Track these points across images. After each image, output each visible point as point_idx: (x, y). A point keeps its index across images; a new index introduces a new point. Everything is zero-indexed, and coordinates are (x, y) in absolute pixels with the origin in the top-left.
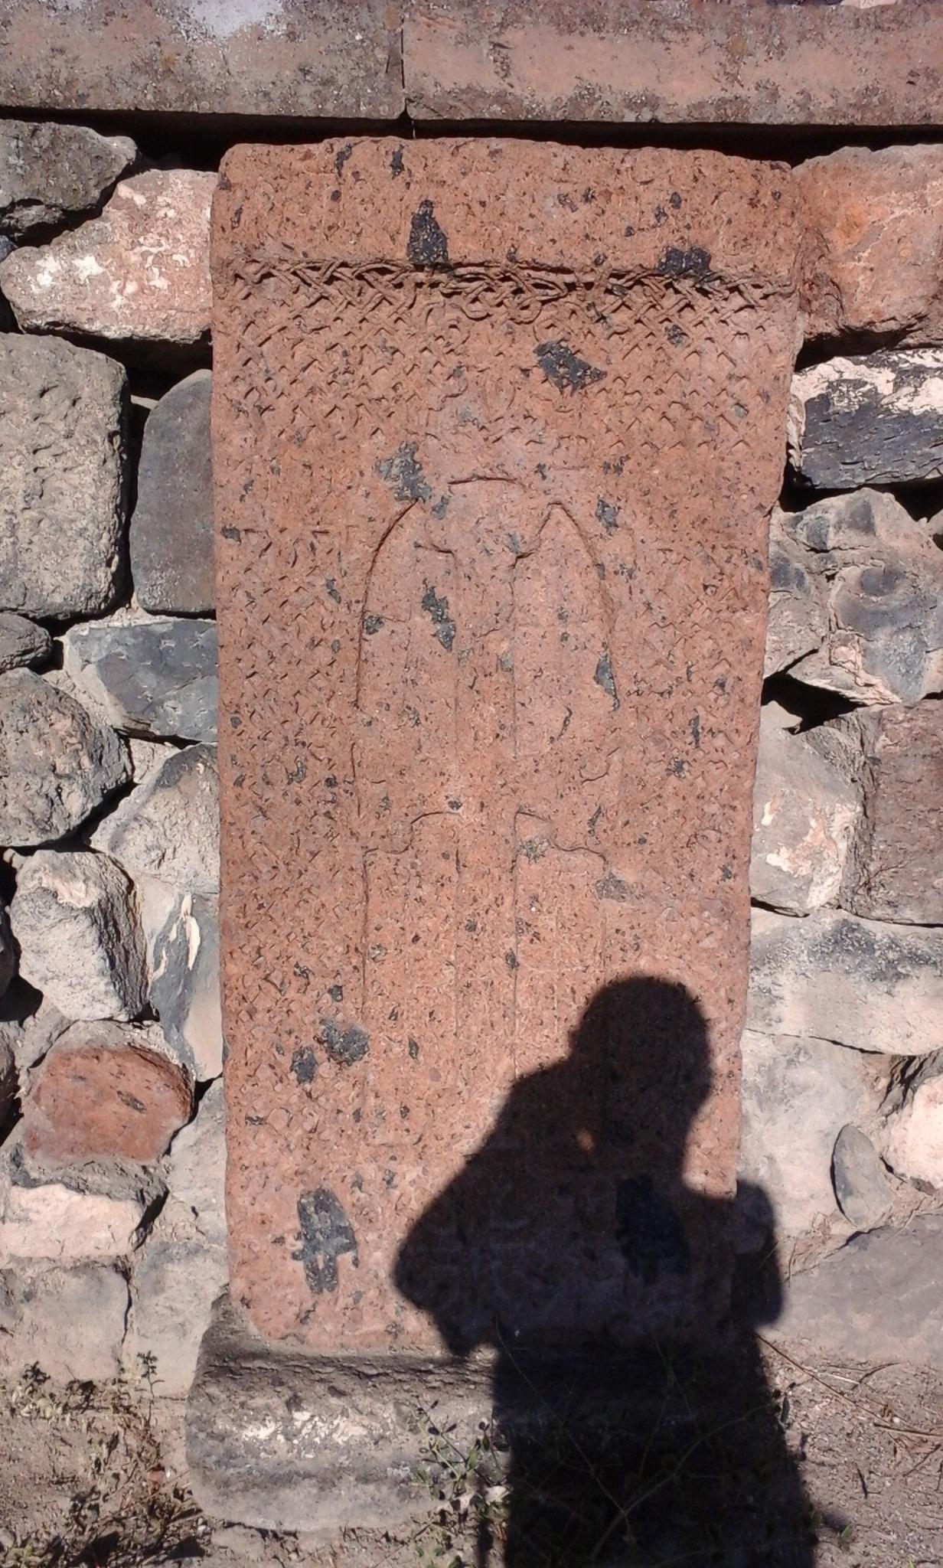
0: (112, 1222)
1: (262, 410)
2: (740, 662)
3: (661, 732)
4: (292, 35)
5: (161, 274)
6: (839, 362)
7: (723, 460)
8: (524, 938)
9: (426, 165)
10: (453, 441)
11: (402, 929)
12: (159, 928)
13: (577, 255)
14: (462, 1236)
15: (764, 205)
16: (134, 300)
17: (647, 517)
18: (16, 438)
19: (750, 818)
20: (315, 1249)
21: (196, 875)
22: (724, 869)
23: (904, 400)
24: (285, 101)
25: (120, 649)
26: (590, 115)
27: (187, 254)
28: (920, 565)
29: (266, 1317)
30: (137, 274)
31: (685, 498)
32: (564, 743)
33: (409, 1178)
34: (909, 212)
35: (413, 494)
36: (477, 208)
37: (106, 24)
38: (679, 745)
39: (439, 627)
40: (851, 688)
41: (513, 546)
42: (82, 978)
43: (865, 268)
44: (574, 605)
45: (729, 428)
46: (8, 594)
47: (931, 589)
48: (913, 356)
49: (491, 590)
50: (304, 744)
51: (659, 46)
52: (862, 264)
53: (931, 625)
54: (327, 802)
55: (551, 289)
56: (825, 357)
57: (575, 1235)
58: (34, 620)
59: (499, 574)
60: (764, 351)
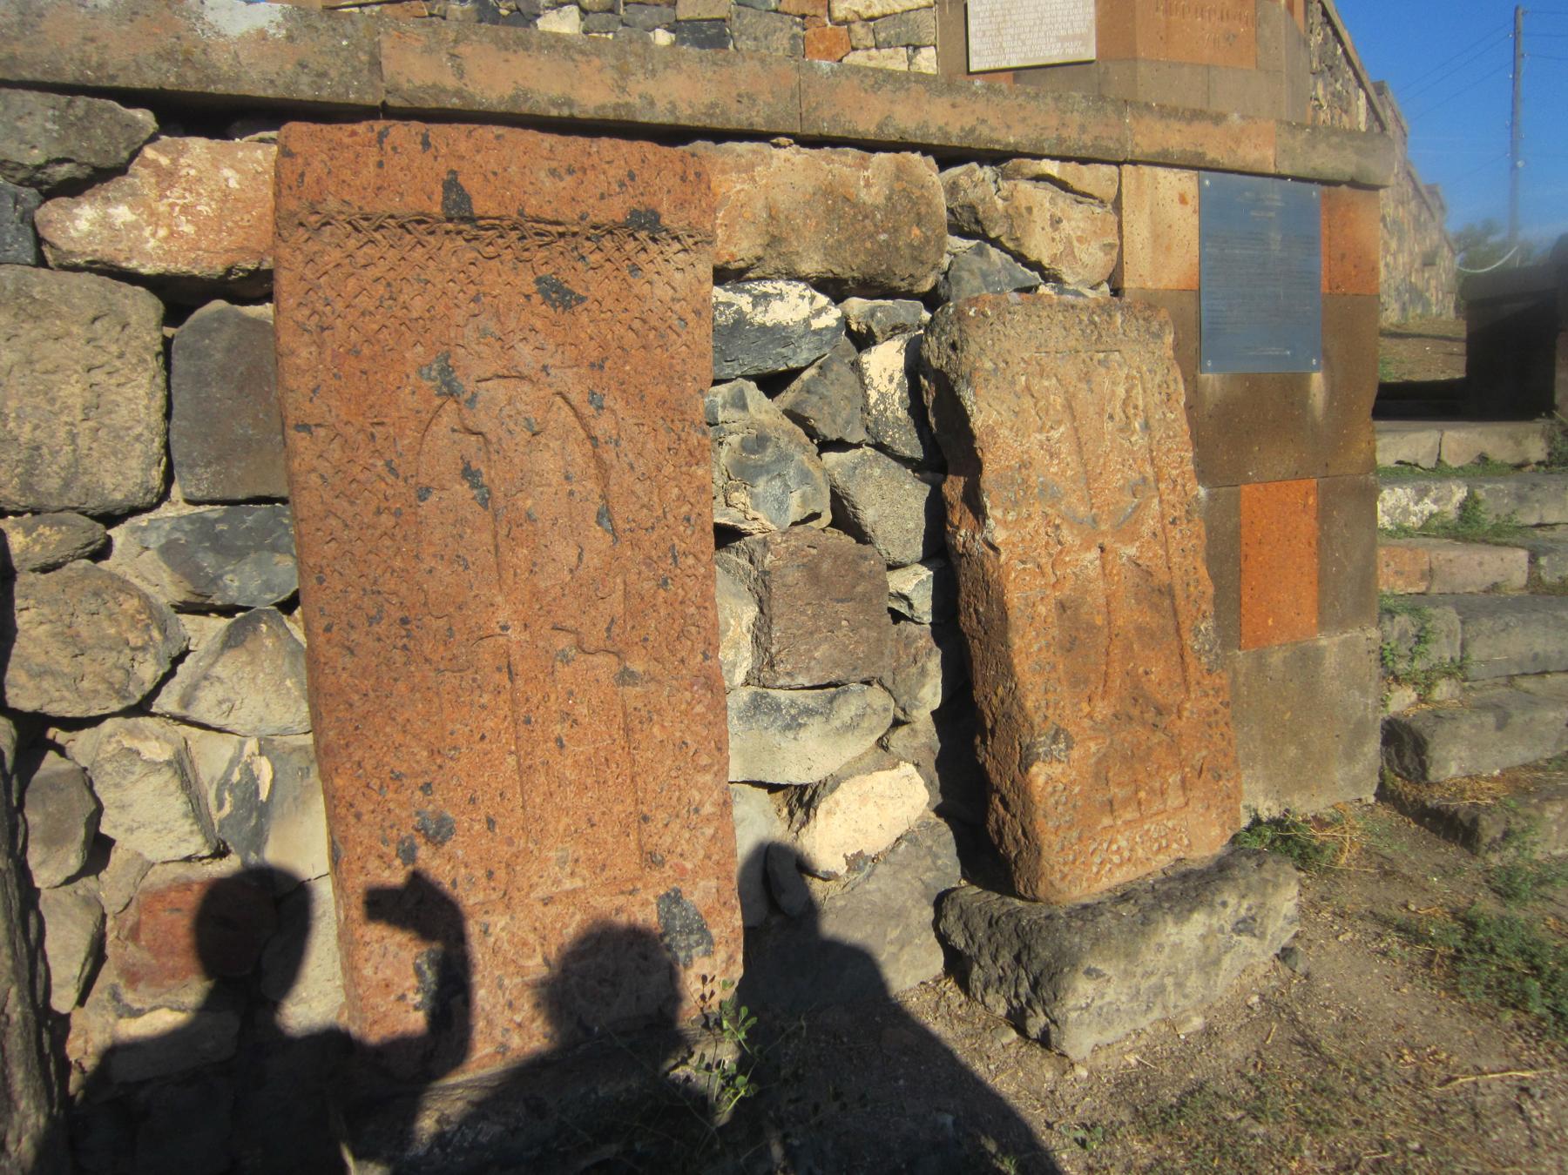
1: (323, 329)
3: (650, 558)
4: (290, 38)
5: (188, 221)
12: (219, 774)
16: (167, 243)
18: (72, 359)
19: (716, 616)
21: (261, 720)
22: (704, 653)
24: (287, 87)
25: (177, 535)
27: (210, 206)
30: (167, 221)
32: (581, 572)
33: (500, 925)
34: (746, 187)
35: (450, 391)
36: (491, 177)
37: (131, 21)
38: (664, 566)
39: (475, 492)
40: (742, 522)
41: (529, 425)
45: (675, 336)
46: (70, 495)
49: (516, 461)
50: (379, 592)
51: (570, 64)
54: (403, 637)
58: (92, 517)
59: (521, 449)
60: (694, 282)
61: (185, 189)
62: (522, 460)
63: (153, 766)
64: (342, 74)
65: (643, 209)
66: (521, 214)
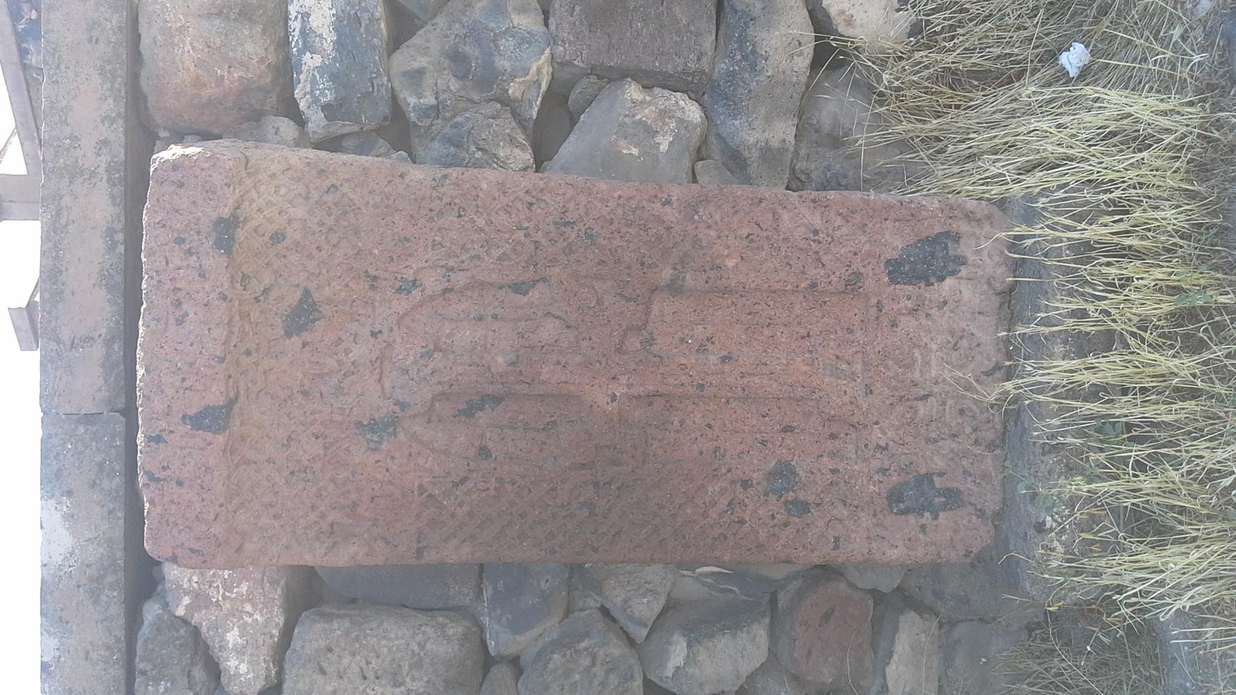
3: (564, 250)
4: (69, 493)
5: (237, 587)
6: (298, 93)
9: (157, 419)
14: (925, 397)
17: (409, 258)
20: (930, 504)
22: (664, 204)
26: (119, 278)
29: (979, 540)
40: (540, 85)
41: (429, 355)
43: (229, 72)
47: (466, 24)
48: (294, 36)
49: (460, 369)
53: (493, 25)
56: (295, 104)
57: (928, 315)
61: (210, 586)
63: (690, 659)
64: (98, 450)
66: (222, 360)
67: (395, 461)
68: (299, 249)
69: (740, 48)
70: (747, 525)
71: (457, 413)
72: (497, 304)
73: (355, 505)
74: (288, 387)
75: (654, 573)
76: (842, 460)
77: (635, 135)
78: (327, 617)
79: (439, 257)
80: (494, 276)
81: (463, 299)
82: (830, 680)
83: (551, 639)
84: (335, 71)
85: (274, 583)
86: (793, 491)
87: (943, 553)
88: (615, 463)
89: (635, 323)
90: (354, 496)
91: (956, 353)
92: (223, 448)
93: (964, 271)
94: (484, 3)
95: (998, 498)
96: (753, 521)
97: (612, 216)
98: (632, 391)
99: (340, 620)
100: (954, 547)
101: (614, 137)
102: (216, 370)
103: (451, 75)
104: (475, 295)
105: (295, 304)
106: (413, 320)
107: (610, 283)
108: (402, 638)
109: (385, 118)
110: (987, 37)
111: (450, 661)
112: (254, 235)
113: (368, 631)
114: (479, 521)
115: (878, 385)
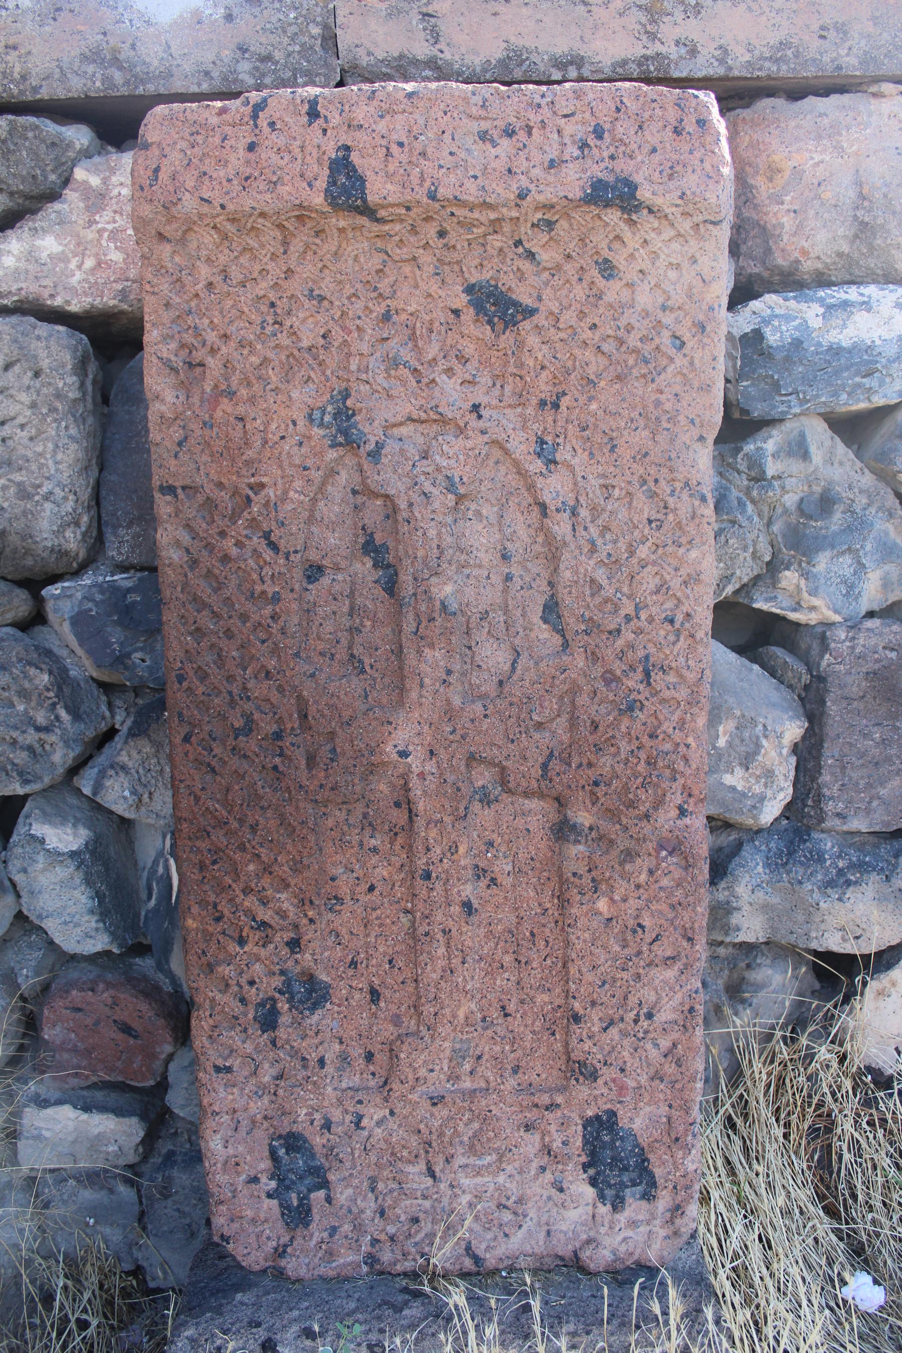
0: (117, 1137)
2: (688, 597)
3: (610, 671)
5: (116, 248)
6: (771, 298)
7: (661, 393)
8: (481, 884)
9: (343, 111)
10: (385, 385)
11: (358, 879)
13: (499, 190)
14: (431, 1173)
15: (689, 133)
16: (93, 274)
17: (587, 453)
20: (288, 1188)
23: (833, 333)
24: (225, 79)
28: (856, 490)
31: (626, 433)
40: (794, 610)
41: (451, 487)
42: (74, 916)
44: (518, 545)
47: (867, 512)
48: (838, 292)
49: (432, 533)
52: (786, 207)
53: (868, 547)
55: (478, 227)
56: (756, 296)
57: (543, 1169)
60: (698, 282)
62: (439, 534)
65: (611, 179)
66: (432, 196)
67: (297, 448)
68: (591, 299)
69: (852, 866)
70: (238, 949)
71: (369, 531)
72: (527, 579)
73: (231, 394)
74: (395, 292)
75: (163, 801)
76: (338, 1069)
77: (742, 741)
78: (81, 367)
79: (591, 495)
80: (568, 574)
81: (532, 531)
82: (46, 1037)
83: (69, 667)
84: (805, 345)
85: (124, 294)
86: (290, 1009)
87: (223, 1208)
88: (311, 761)
89: (511, 778)
90: (244, 392)
91: (494, 1207)
92: (306, 204)
93: (604, 1210)
94: (892, 534)
95: (303, 1272)
96: (245, 957)
97: (660, 738)
98: (414, 782)
99: (77, 385)
100: (232, 1221)
101: (738, 713)
102: (417, 189)
103: (801, 495)
104: (538, 548)
105: (514, 297)
106: (497, 462)
107: (565, 738)
108: (57, 470)
109: (746, 412)
110: (875, 1167)
111: (31, 537)
112: (611, 237)
113: (63, 424)
114: (218, 572)
115: (445, 1113)
